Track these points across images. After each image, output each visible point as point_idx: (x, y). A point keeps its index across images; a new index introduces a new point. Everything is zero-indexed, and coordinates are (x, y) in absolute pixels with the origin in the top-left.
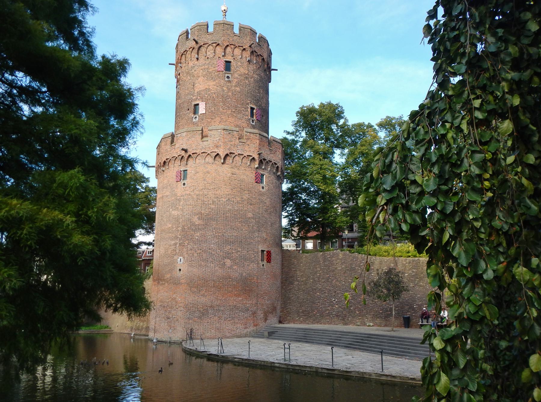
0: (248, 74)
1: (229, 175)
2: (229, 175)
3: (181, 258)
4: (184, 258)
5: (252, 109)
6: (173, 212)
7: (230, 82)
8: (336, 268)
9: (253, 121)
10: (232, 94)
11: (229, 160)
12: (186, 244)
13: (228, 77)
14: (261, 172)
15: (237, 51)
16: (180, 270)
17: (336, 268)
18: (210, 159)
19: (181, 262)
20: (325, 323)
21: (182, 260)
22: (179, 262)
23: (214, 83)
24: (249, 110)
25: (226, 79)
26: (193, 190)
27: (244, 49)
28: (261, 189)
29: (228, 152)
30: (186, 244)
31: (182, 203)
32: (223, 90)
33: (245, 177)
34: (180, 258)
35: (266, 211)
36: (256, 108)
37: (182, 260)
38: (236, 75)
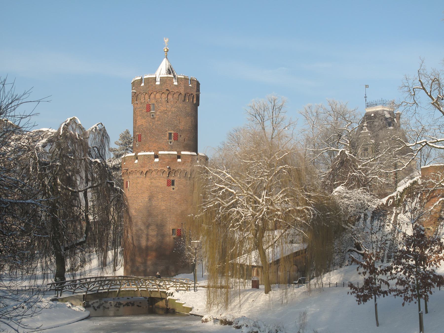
0: (166, 110)
1: (149, 184)
2: (149, 184)
5: (170, 134)
7: (154, 118)
9: (171, 143)
10: (156, 126)
11: (148, 175)
13: (153, 115)
14: (172, 179)
15: (158, 96)
18: (138, 175)
23: (145, 120)
24: (168, 135)
25: (152, 117)
27: (163, 93)
28: (172, 190)
29: (148, 169)
32: (150, 125)
33: (160, 184)
35: (176, 203)
36: (173, 132)
38: (158, 113)
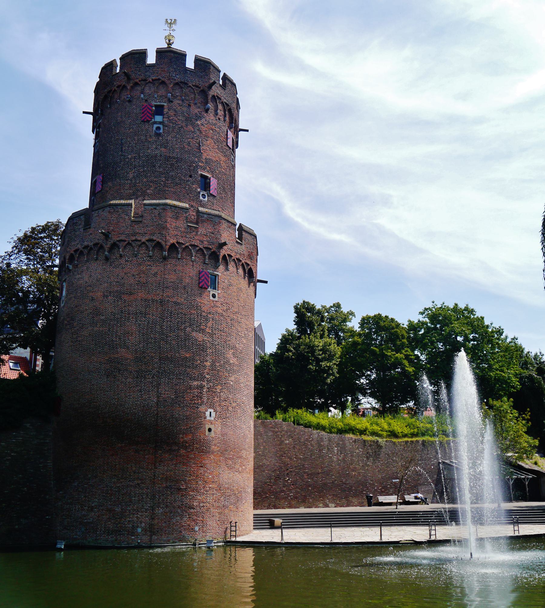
3: (212, 410)
4: (215, 411)
6: (194, 334)
8: (283, 441)
12: (218, 391)
16: (210, 430)
17: (283, 441)
19: (212, 419)
20: (283, 508)
21: (213, 414)
22: (208, 418)
26: (227, 310)
30: (218, 391)
31: (210, 324)
34: (210, 410)
37: (213, 414)
